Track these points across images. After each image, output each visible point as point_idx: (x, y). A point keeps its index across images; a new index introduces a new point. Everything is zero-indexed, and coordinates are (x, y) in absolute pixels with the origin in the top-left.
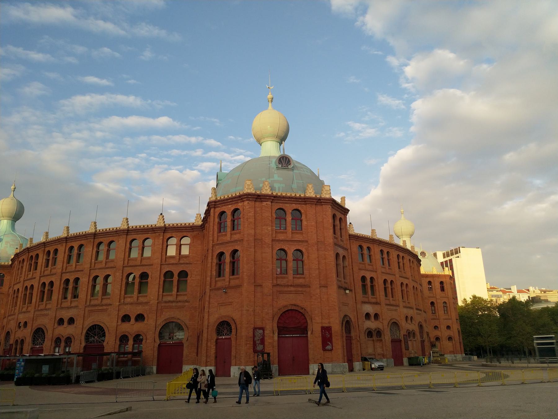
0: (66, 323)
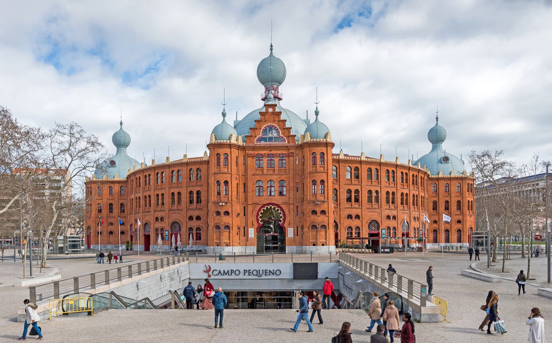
0: (160, 220)
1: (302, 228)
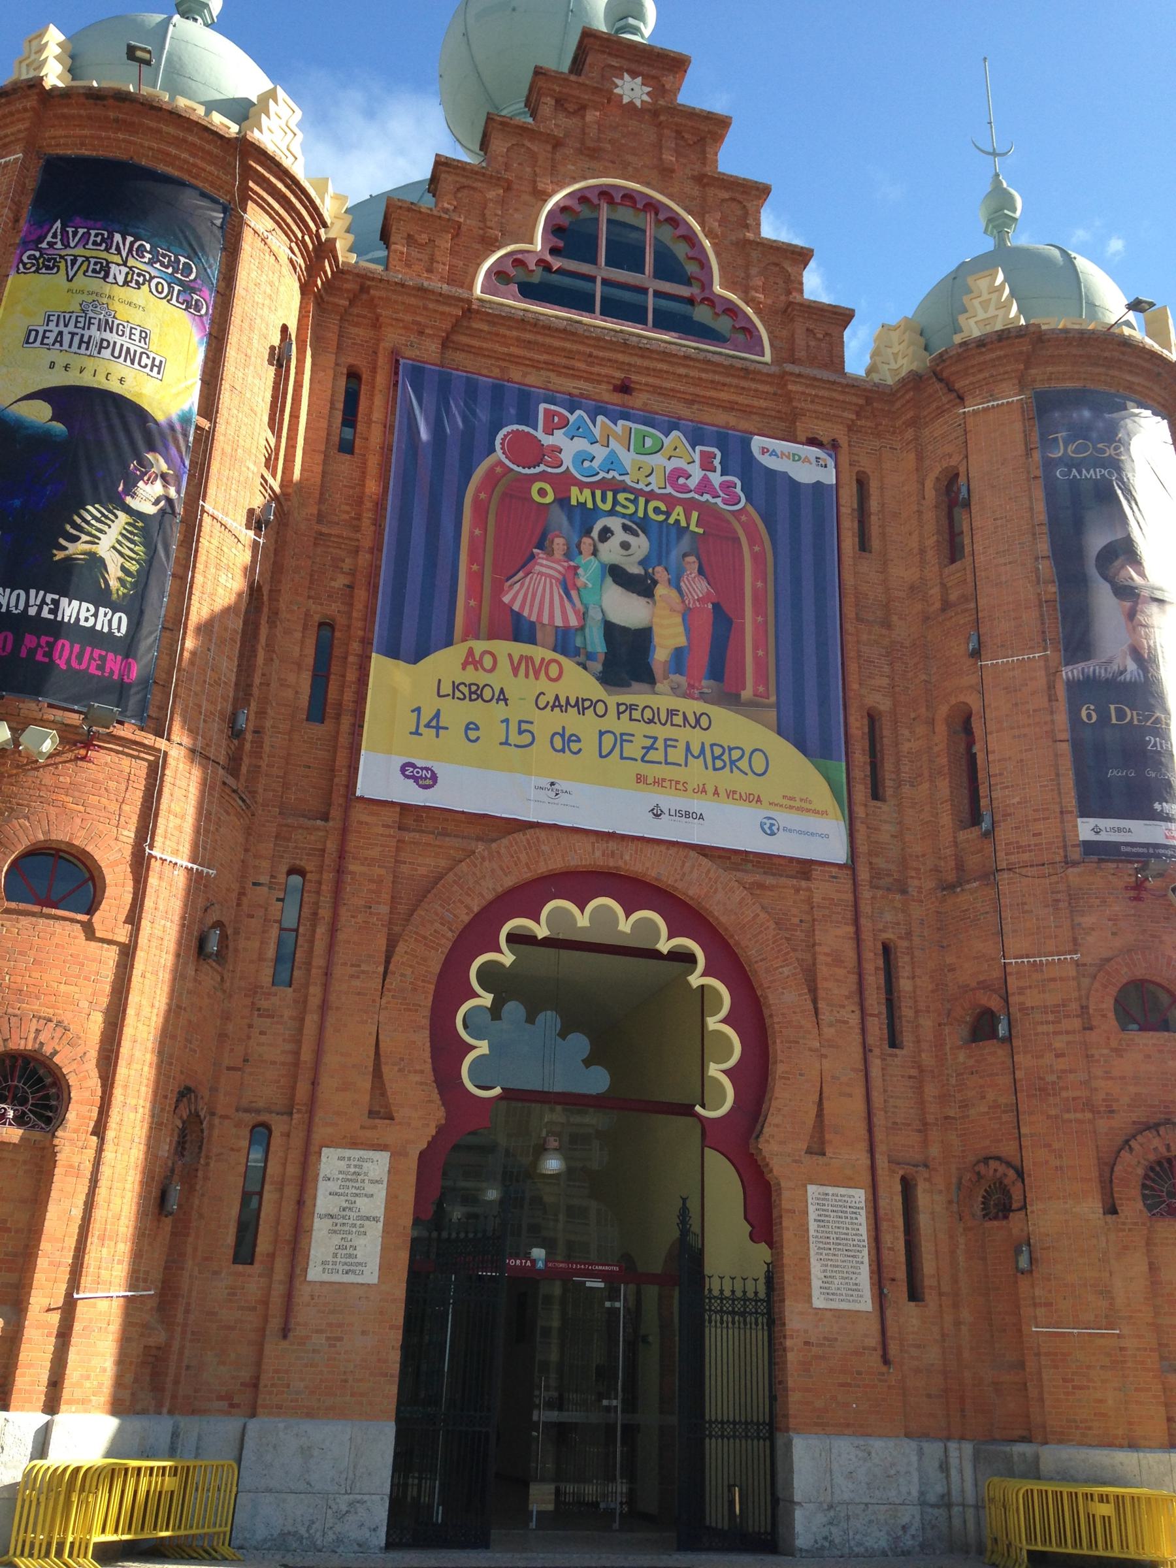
1: (997, 1195)
